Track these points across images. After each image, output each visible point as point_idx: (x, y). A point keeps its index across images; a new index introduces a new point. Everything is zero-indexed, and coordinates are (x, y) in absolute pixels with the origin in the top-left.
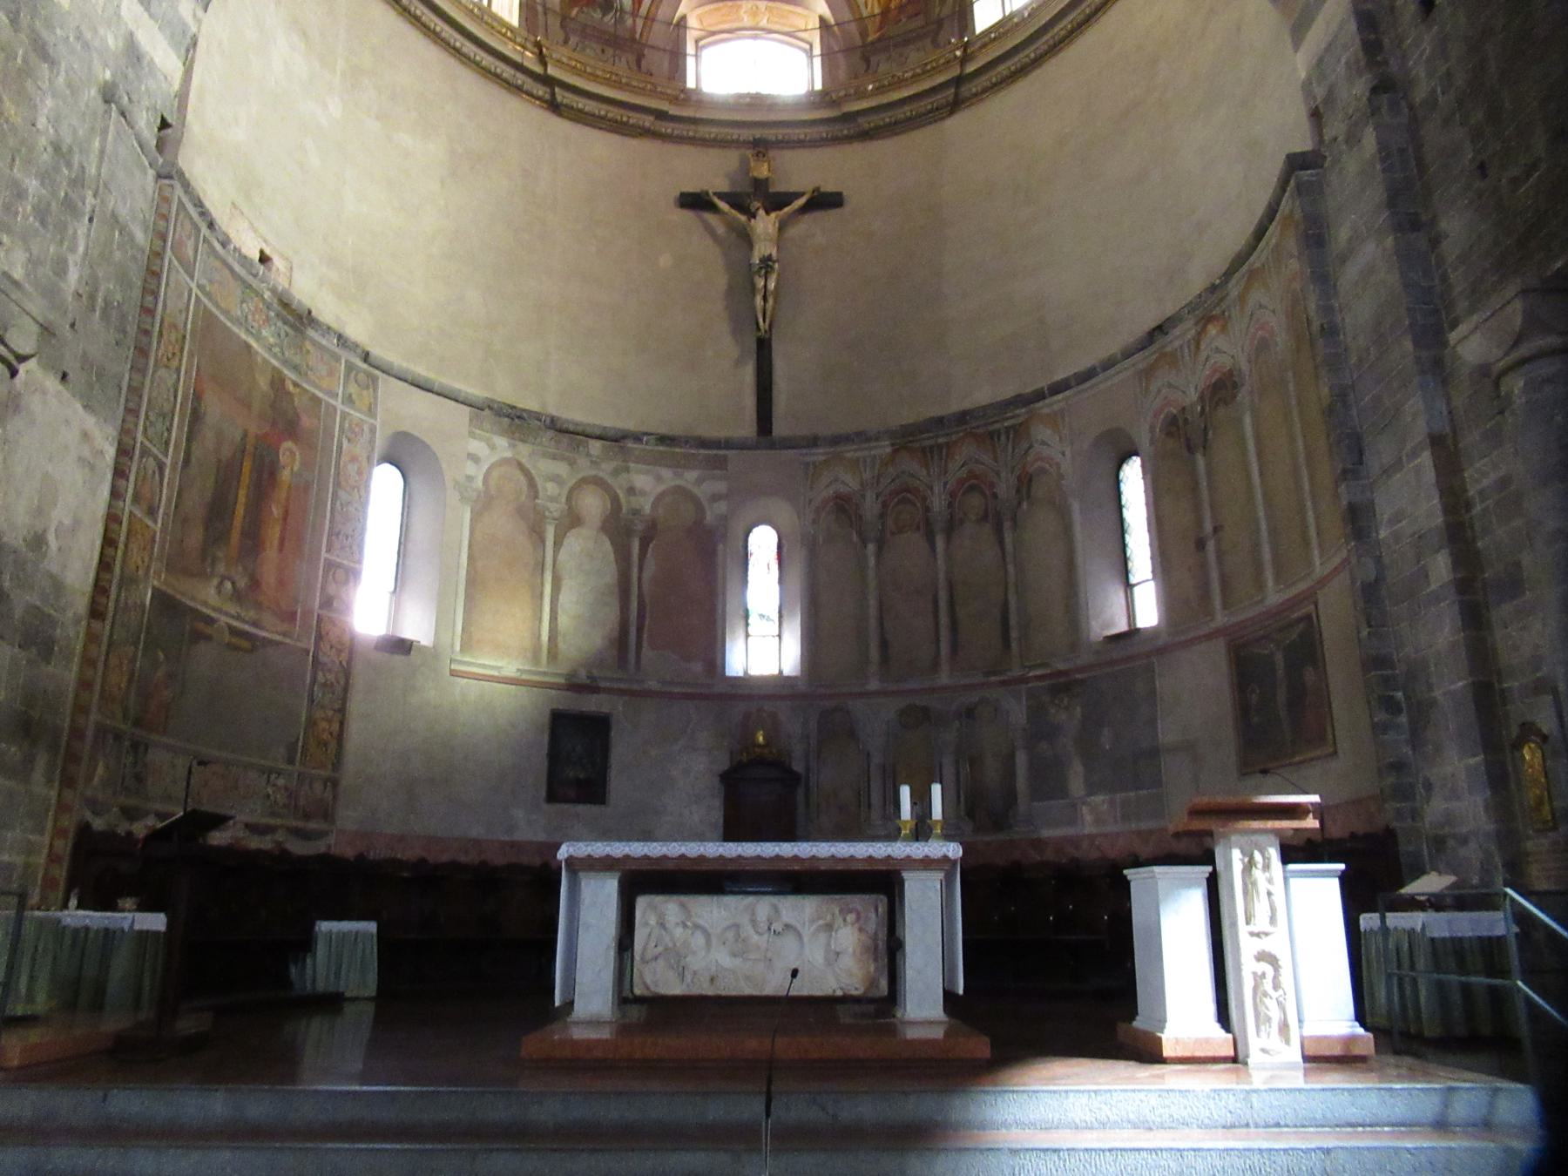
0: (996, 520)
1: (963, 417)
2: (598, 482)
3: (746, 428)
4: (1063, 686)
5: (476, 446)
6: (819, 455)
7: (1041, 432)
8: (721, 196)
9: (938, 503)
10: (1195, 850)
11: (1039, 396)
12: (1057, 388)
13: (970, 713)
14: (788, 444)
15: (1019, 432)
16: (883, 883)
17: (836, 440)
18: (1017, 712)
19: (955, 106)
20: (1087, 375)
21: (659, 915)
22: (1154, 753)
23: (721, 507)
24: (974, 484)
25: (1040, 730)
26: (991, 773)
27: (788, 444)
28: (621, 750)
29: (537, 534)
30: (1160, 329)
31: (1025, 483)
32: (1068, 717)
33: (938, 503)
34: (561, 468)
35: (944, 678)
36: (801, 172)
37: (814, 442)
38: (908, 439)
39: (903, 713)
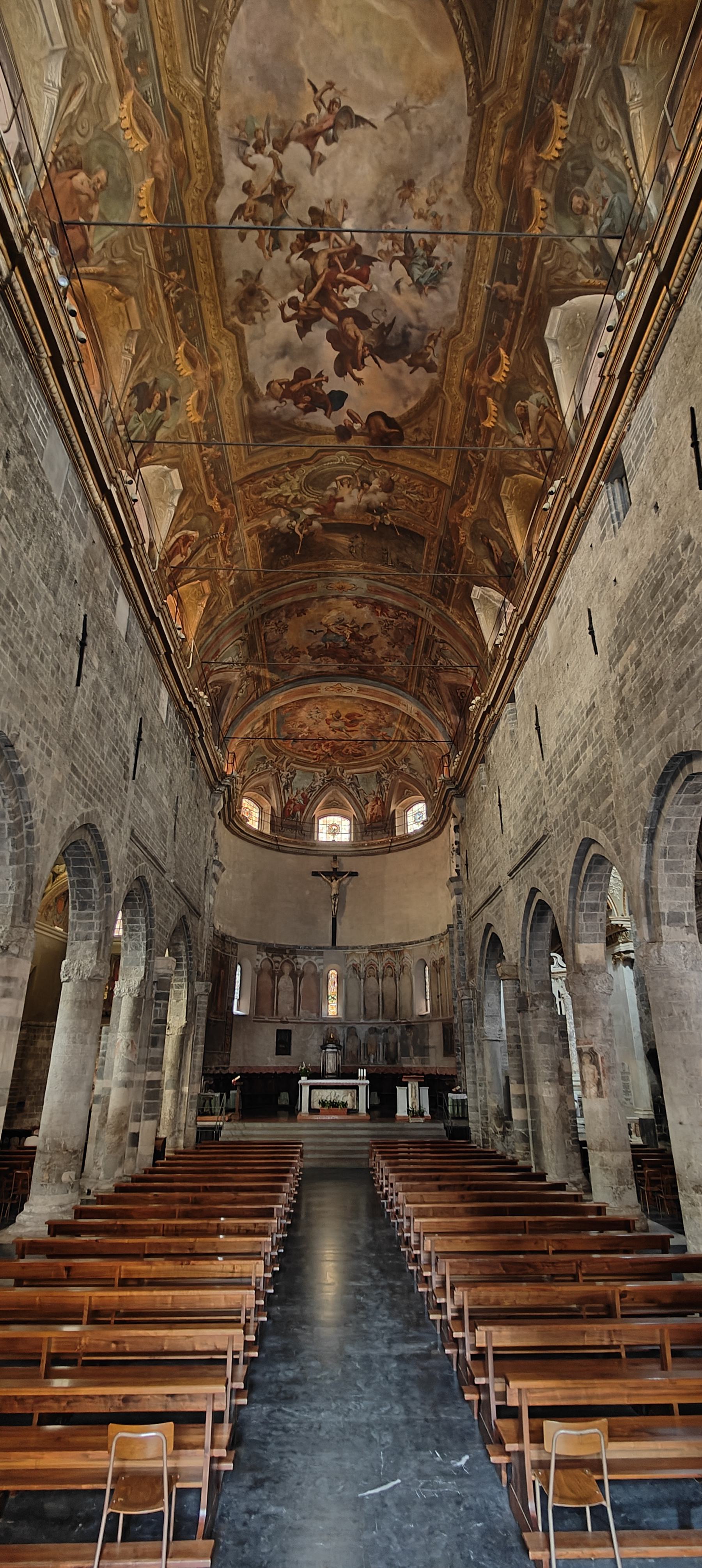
0: (395, 977)
1: (387, 945)
2: (288, 961)
3: (330, 944)
4: (409, 1026)
5: (259, 957)
6: (349, 951)
7: (406, 954)
8: (323, 873)
9: (380, 969)
10: (406, 1084)
11: (406, 944)
12: (411, 943)
13: (386, 1031)
14: (340, 948)
15: (401, 953)
16: (356, 1087)
17: (354, 948)
18: (398, 1032)
19: (389, 852)
20: (418, 942)
21: (316, 1092)
22: (428, 1047)
23: (321, 967)
24: (389, 966)
25: (403, 1037)
26: (391, 1049)
27: (340, 948)
28: (294, 1039)
29: (273, 978)
30: (432, 938)
31: (402, 967)
32: (410, 1034)
33: (380, 969)
34: (279, 959)
35: (380, 1021)
36: (347, 864)
37: (347, 948)
38: (372, 949)
39: (370, 1029)
